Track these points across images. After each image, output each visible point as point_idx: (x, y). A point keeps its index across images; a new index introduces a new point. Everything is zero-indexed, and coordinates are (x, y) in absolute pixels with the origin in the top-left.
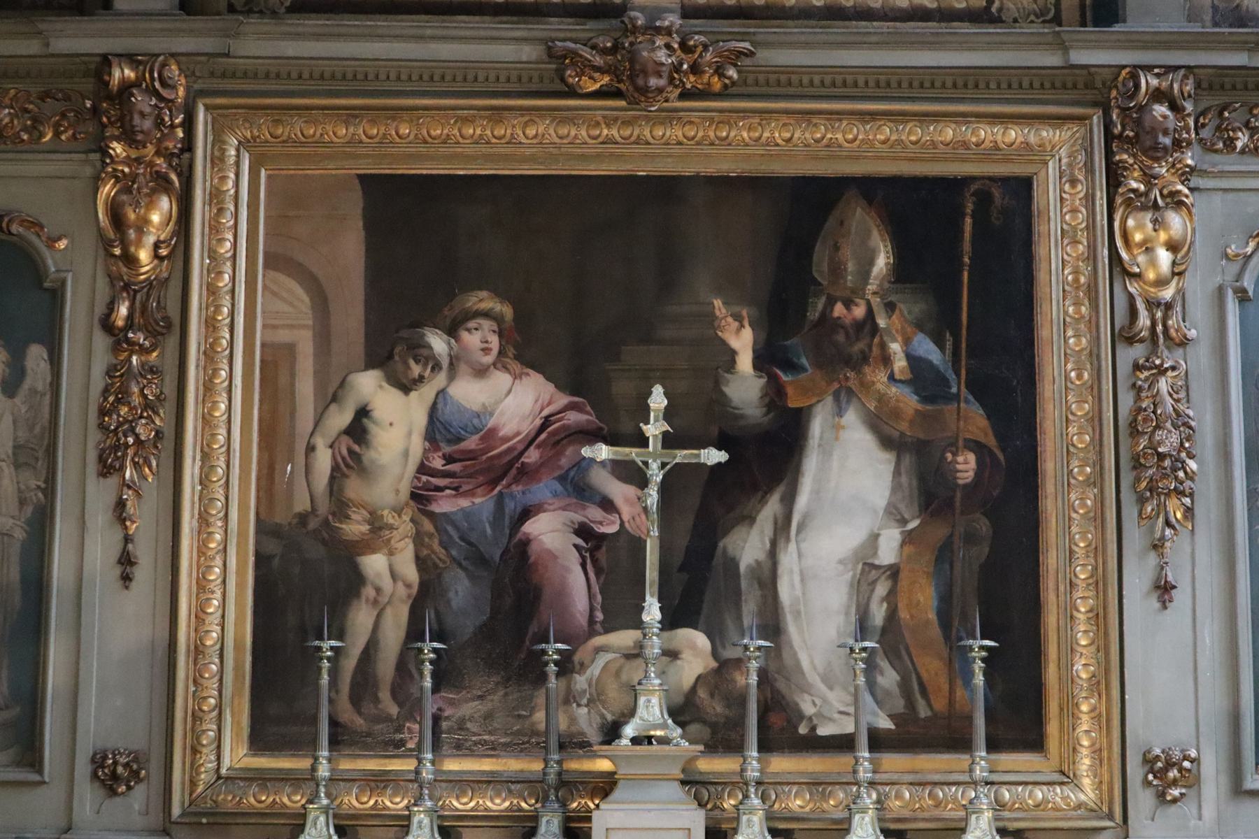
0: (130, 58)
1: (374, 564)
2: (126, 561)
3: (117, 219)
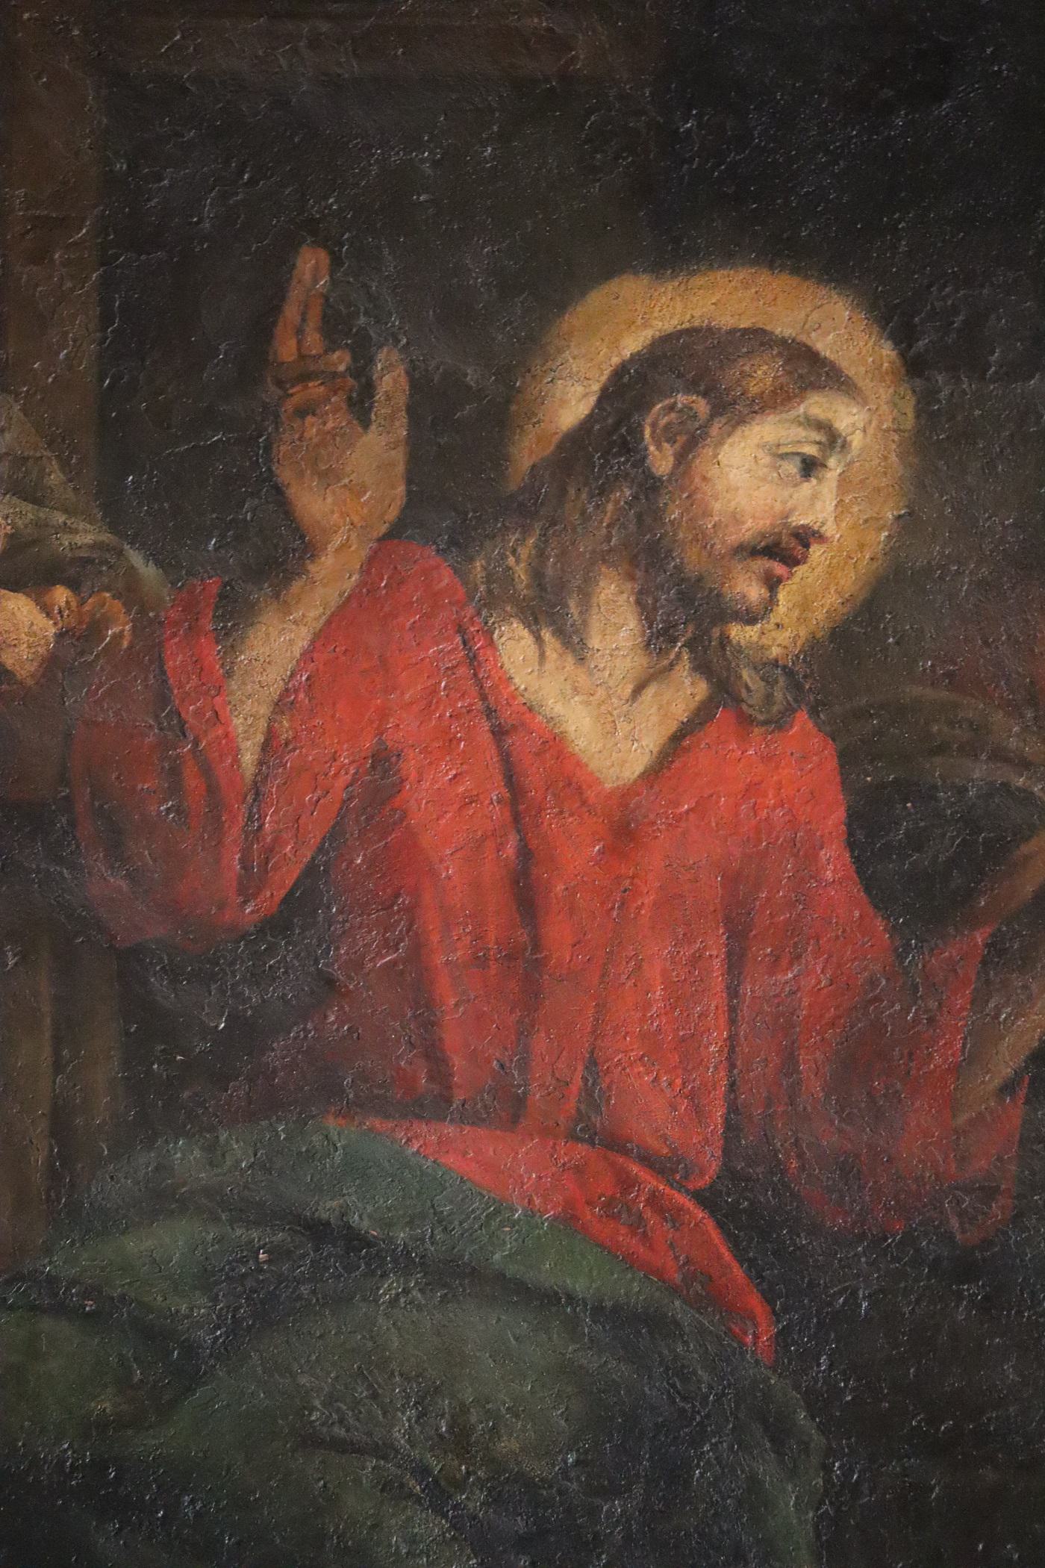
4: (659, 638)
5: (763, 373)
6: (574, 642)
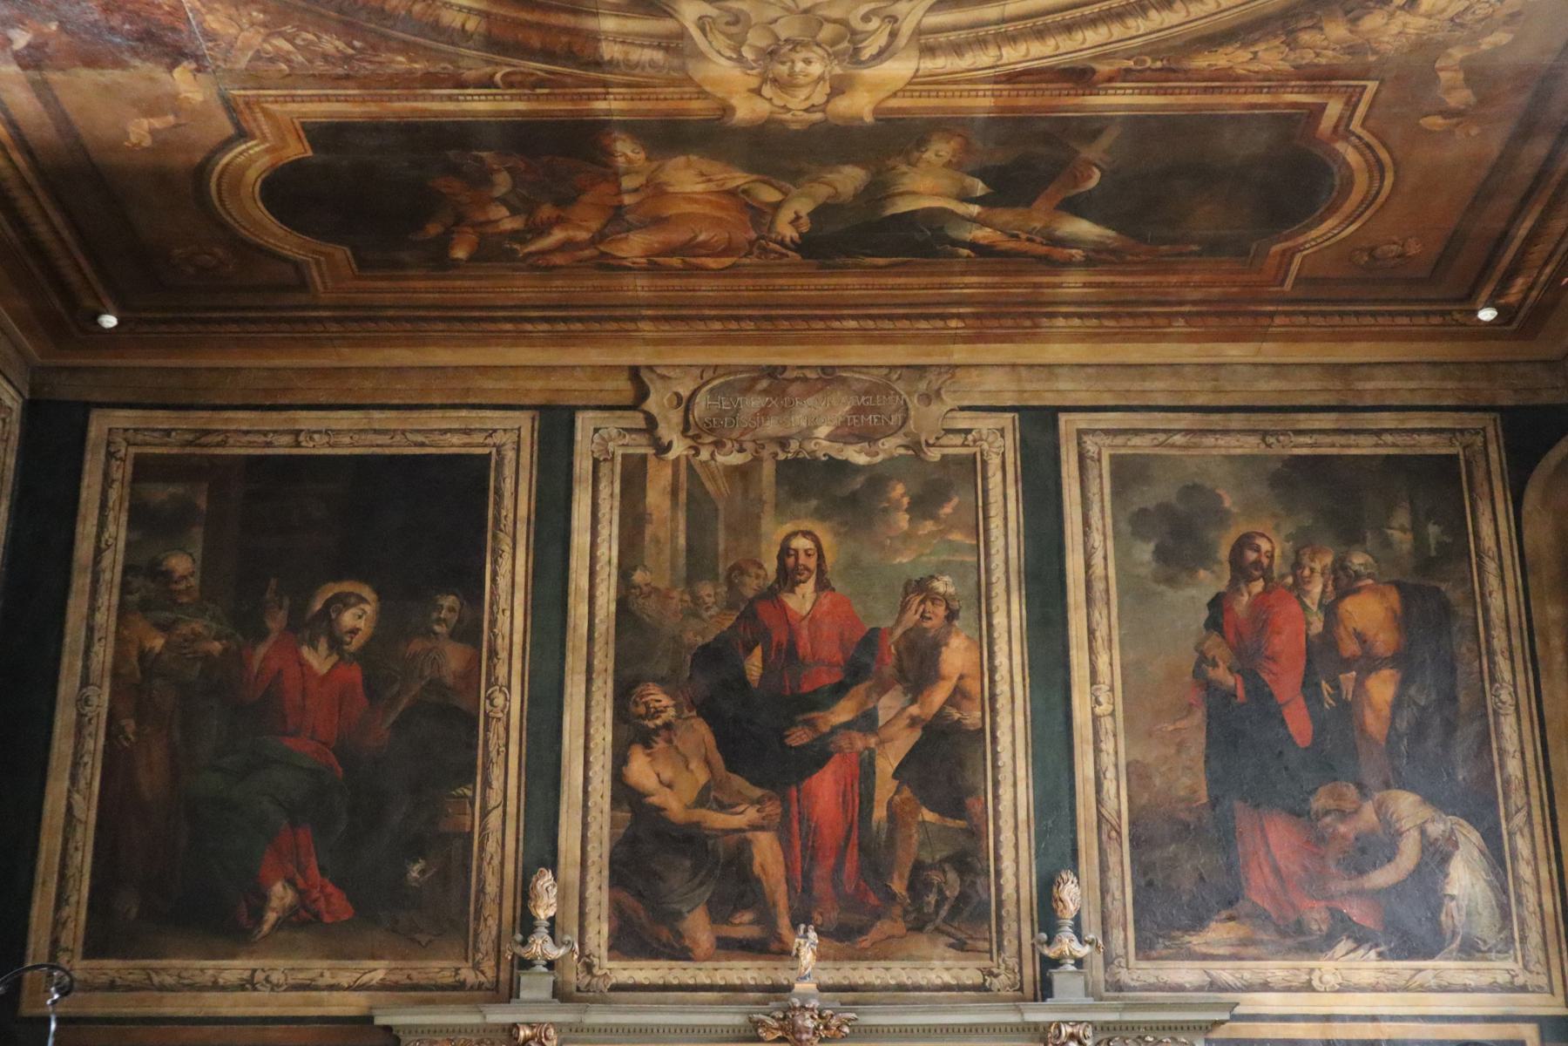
0: (530, 1025)
4: (331, 648)
5: (353, 600)
6: (316, 649)
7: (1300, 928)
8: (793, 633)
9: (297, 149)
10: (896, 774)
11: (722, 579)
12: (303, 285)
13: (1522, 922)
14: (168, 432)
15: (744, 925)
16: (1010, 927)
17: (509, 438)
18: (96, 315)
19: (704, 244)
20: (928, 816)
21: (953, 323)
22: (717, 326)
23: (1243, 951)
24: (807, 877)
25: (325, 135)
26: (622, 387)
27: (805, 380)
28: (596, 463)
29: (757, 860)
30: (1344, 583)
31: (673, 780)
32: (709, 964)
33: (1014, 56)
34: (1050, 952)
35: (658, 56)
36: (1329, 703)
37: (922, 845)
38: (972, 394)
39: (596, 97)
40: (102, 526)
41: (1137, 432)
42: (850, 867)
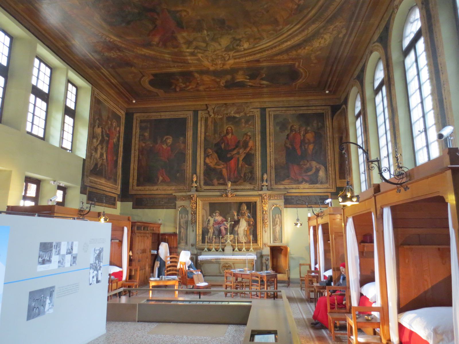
0: (193, 195)
1: (210, 230)
2: (193, 230)
3: (192, 206)
7: (298, 180)
8: (228, 141)
9: (152, 77)
10: (242, 160)
11: (219, 133)
12: (158, 95)
13: (329, 179)
14: (144, 116)
15: (221, 181)
16: (257, 181)
17: (189, 115)
18: (132, 101)
19: (211, 87)
20: (247, 166)
21: (249, 96)
22: (216, 98)
23: (290, 184)
24: (230, 174)
25: (155, 75)
26: (205, 107)
27: (230, 105)
28: (201, 118)
29: (223, 172)
30: (306, 132)
31: (212, 162)
32: (217, 186)
33: (248, 59)
34: (263, 184)
35: (197, 62)
36: (303, 149)
37: (246, 170)
38: (254, 106)
39: (190, 68)
40: (136, 129)
41: (277, 111)
42: (236, 172)
